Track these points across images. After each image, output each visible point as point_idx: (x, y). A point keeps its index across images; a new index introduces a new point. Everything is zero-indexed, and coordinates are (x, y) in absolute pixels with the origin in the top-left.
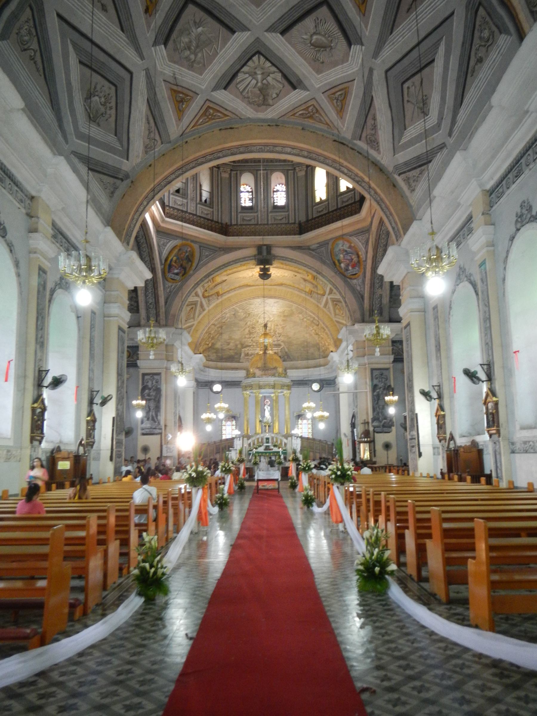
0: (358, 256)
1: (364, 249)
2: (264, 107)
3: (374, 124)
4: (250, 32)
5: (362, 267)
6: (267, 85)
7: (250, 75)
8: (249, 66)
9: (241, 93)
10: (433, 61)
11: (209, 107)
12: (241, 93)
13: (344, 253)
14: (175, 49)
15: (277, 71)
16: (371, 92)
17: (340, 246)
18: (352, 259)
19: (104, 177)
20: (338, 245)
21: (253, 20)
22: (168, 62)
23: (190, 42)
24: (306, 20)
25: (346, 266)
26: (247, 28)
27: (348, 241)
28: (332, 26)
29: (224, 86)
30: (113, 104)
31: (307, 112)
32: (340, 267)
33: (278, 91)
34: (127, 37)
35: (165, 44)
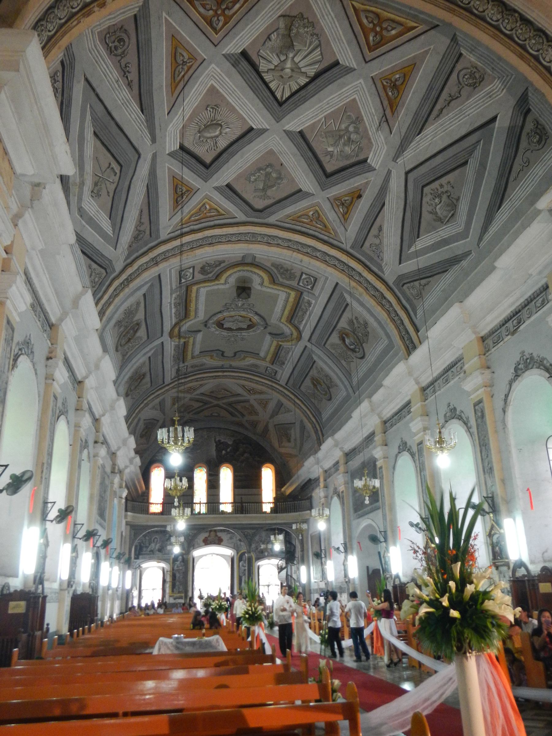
2: (294, 13)
3: (127, 77)
4: (284, 129)
6: (281, 52)
7: (300, 68)
8: (298, 84)
9: (320, 45)
10: (110, 219)
11: (371, 49)
12: (320, 45)
14: (361, 149)
15: (263, 75)
16: (146, 116)
19: (516, 167)
21: (278, 139)
22: (374, 146)
23: (344, 145)
24: (225, 145)
26: (286, 133)
28: (200, 151)
29: (337, 67)
30: (436, 185)
31: (227, 12)
33: (269, 44)
34: (385, 196)
35: (365, 160)
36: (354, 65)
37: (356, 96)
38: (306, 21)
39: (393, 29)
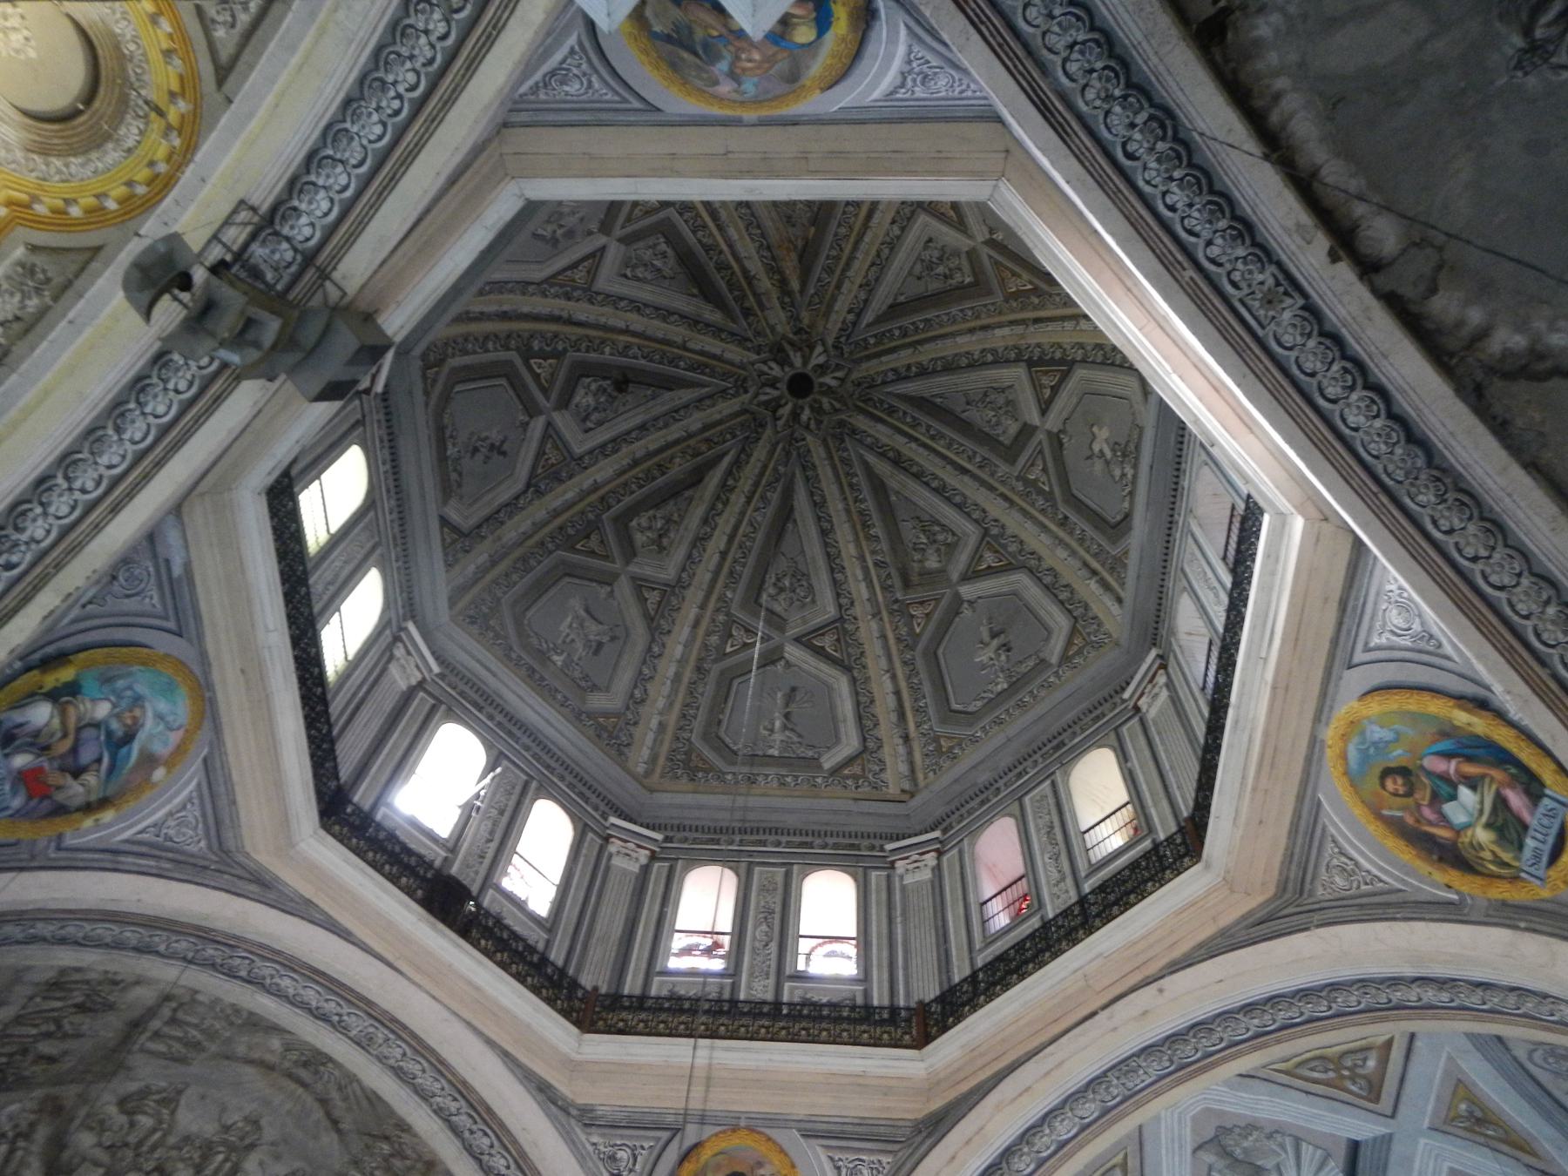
0: (89, 808)
1: (126, 835)
2: (1209, 1133)
5: (24, 832)
11: (1377, 1100)
13: (115, 725)
17: (163, 706)
18: (77, 773)
20: (168, 690)
25: (37, 734)
27: (180, 750)
32: (32, 696)
36: (1383, 1130)
37: (1446, 1165)
38: (1237, 1130)
39: (1365, 1060)
